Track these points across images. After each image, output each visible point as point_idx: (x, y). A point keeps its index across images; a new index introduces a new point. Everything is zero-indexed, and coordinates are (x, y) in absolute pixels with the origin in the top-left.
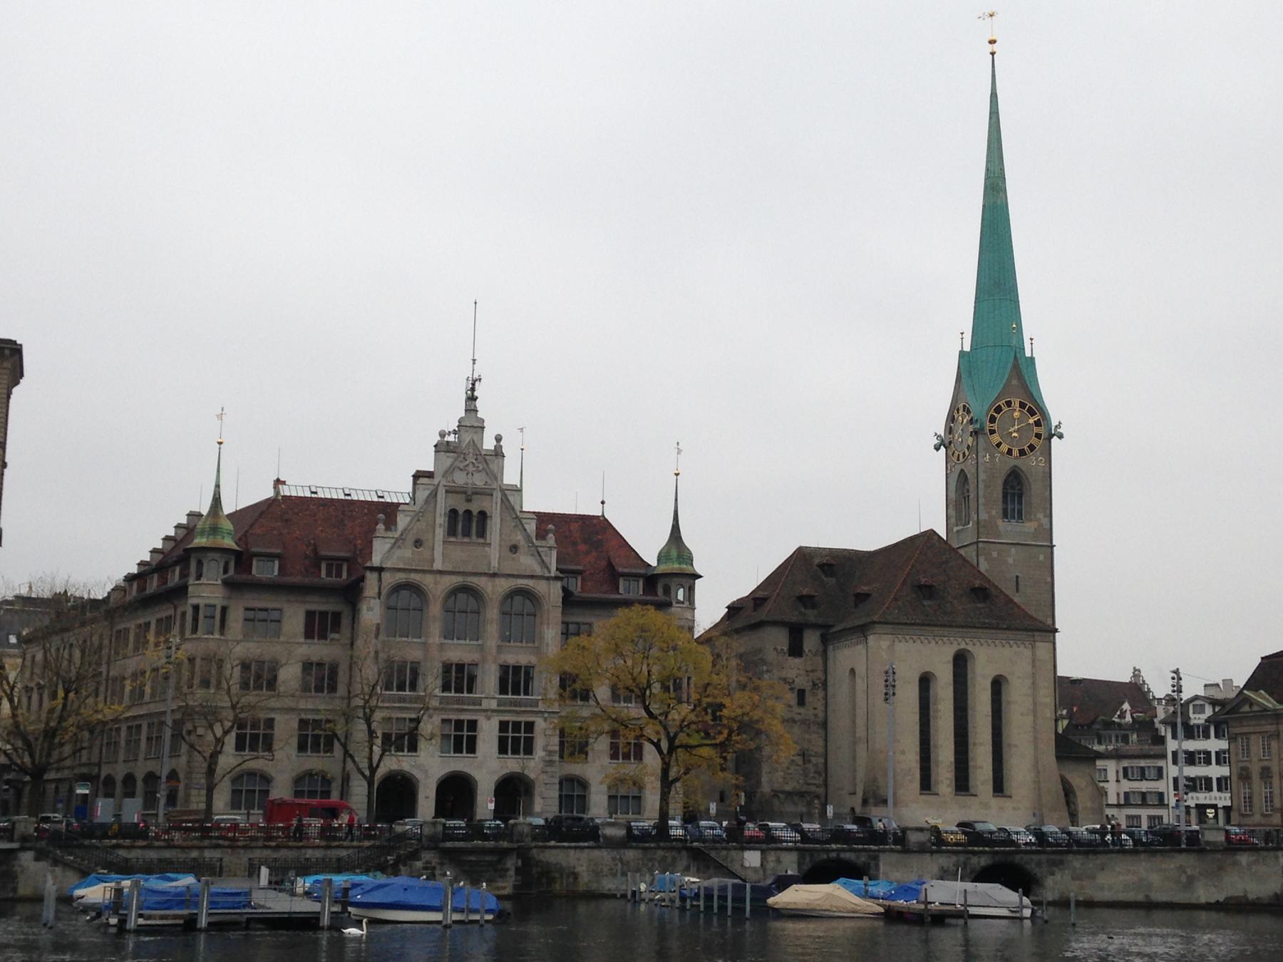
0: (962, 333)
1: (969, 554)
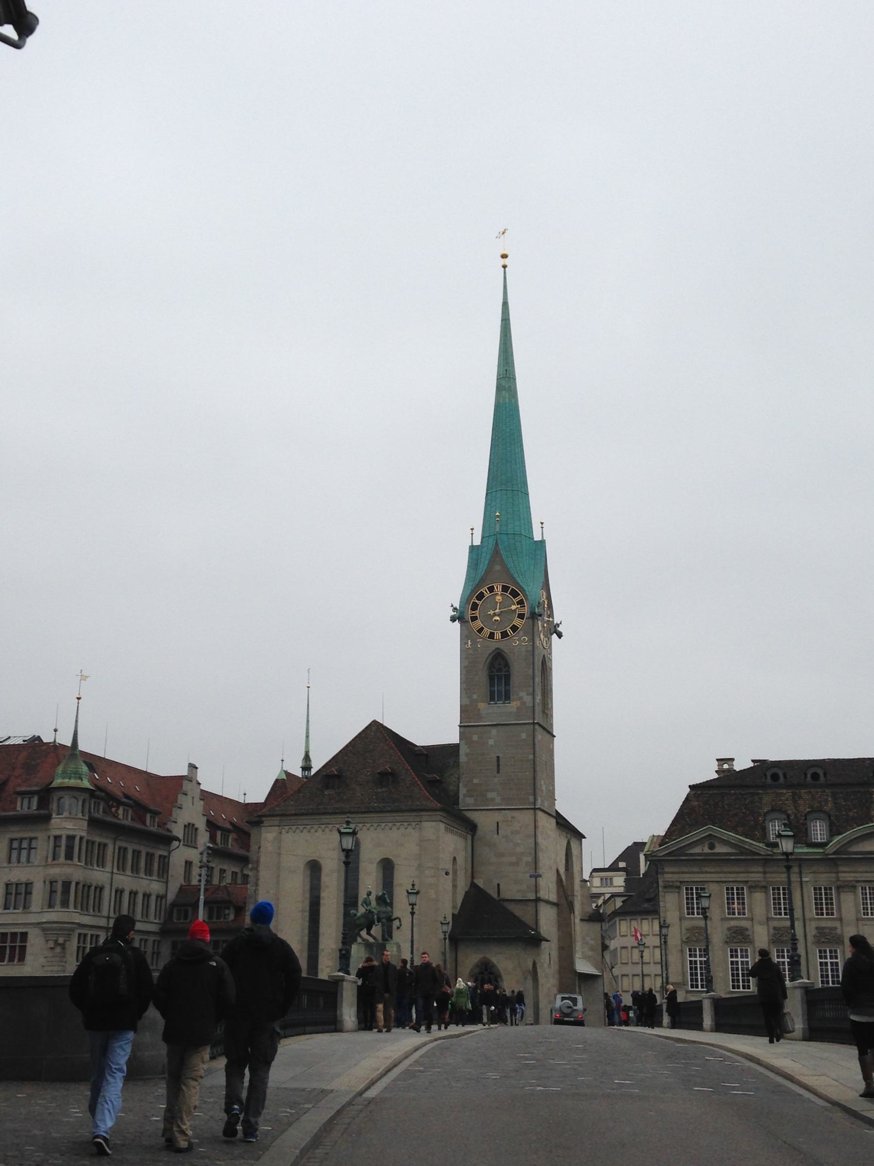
0: (472, 529)
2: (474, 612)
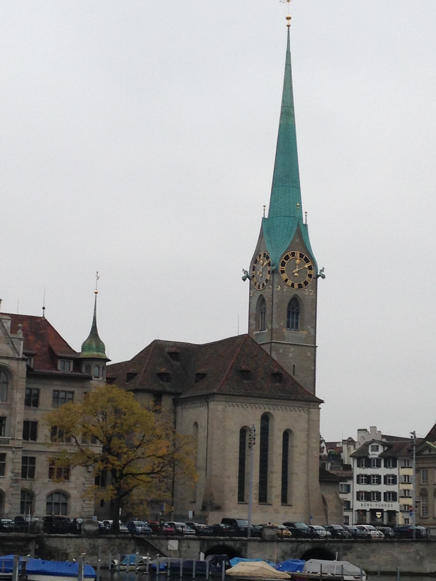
1: (266, 348)
2: (282, 267)
